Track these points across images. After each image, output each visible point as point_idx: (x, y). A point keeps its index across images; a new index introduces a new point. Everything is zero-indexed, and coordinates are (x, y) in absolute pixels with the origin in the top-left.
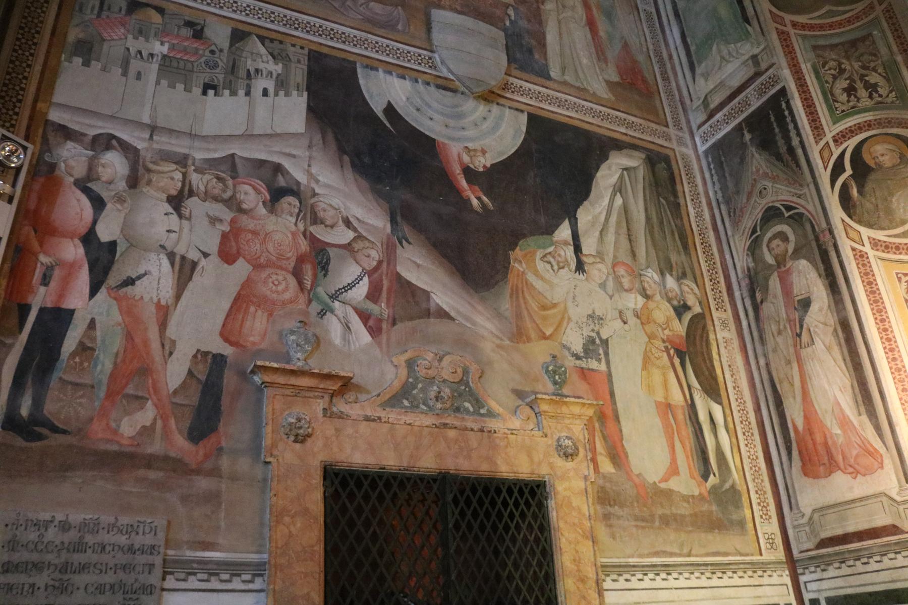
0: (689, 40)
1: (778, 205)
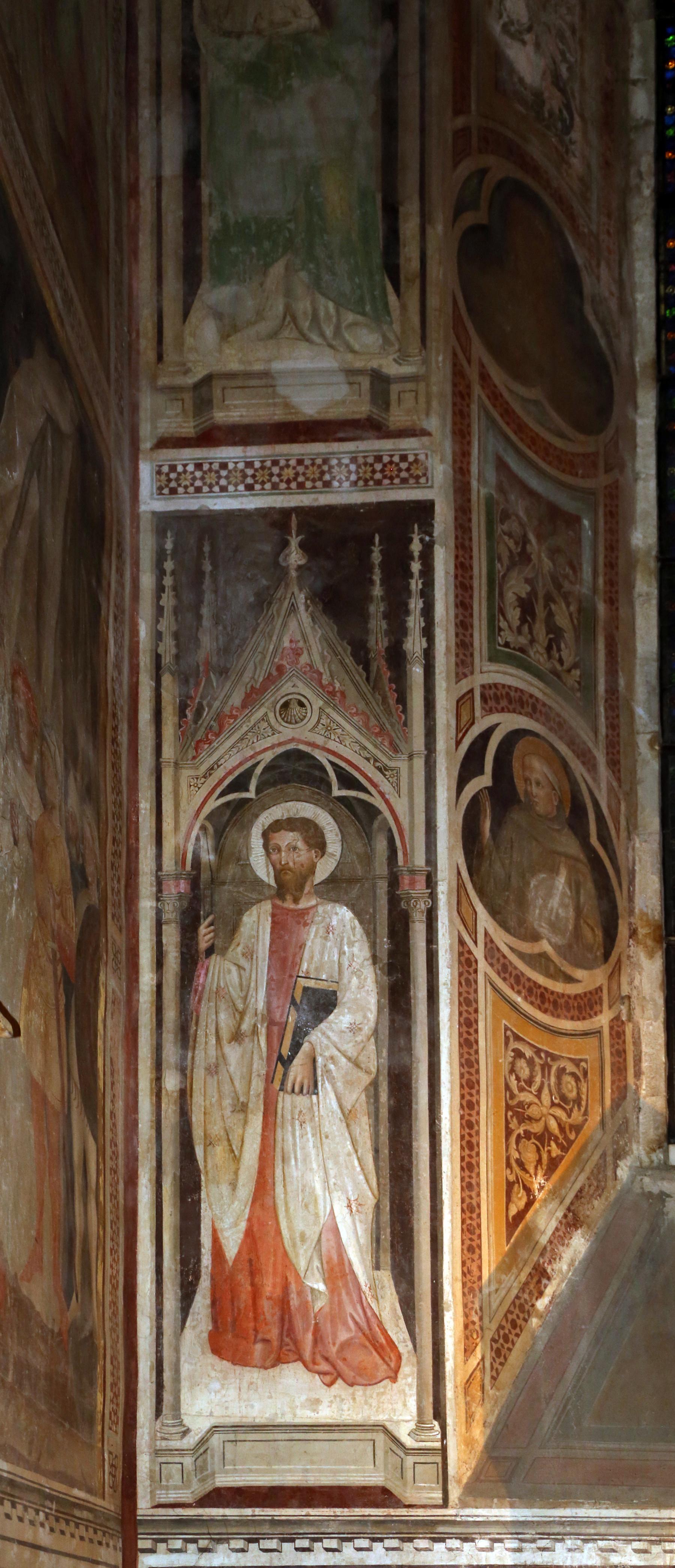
0: (206, 190)
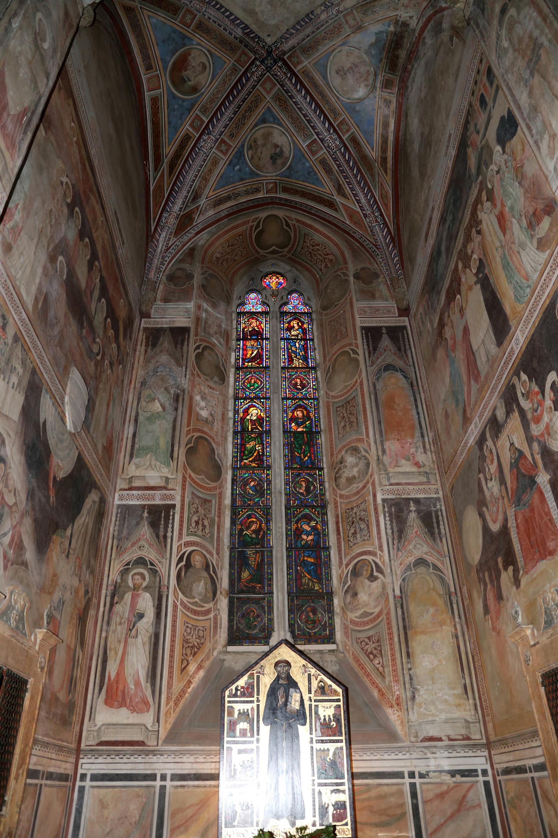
0: (136, 440)
1: (147, 559)
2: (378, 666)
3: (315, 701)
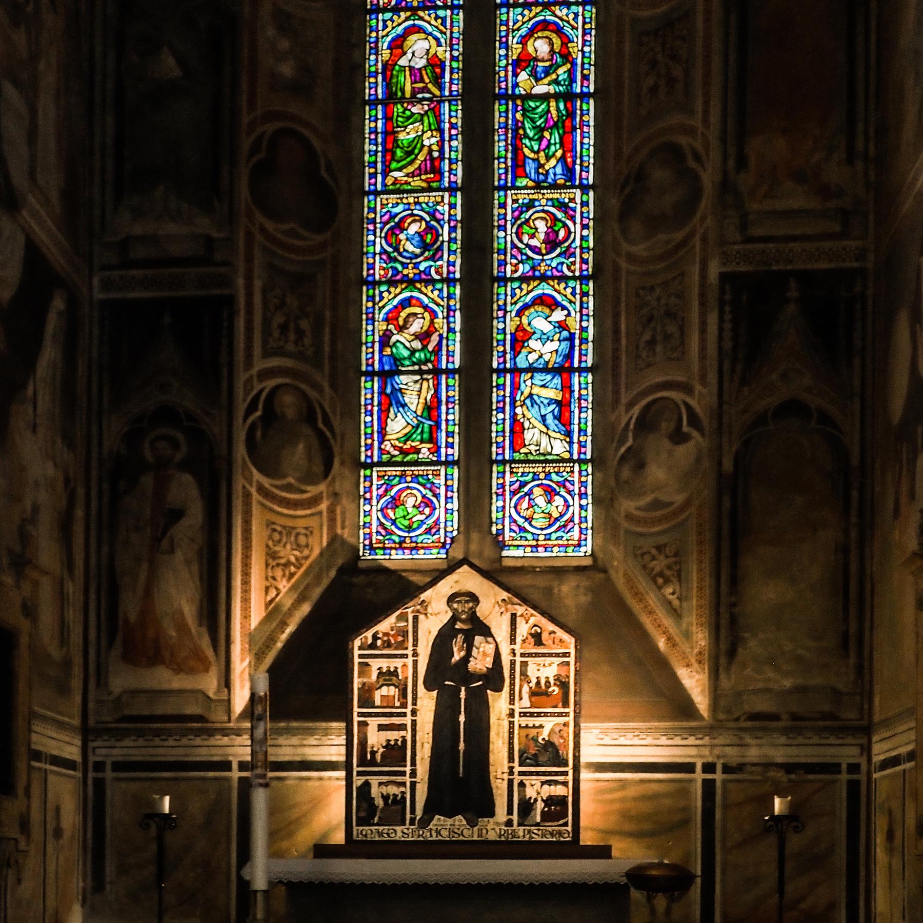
2: (671, 597)
3: (522, 655)
